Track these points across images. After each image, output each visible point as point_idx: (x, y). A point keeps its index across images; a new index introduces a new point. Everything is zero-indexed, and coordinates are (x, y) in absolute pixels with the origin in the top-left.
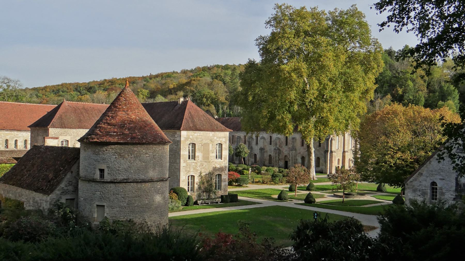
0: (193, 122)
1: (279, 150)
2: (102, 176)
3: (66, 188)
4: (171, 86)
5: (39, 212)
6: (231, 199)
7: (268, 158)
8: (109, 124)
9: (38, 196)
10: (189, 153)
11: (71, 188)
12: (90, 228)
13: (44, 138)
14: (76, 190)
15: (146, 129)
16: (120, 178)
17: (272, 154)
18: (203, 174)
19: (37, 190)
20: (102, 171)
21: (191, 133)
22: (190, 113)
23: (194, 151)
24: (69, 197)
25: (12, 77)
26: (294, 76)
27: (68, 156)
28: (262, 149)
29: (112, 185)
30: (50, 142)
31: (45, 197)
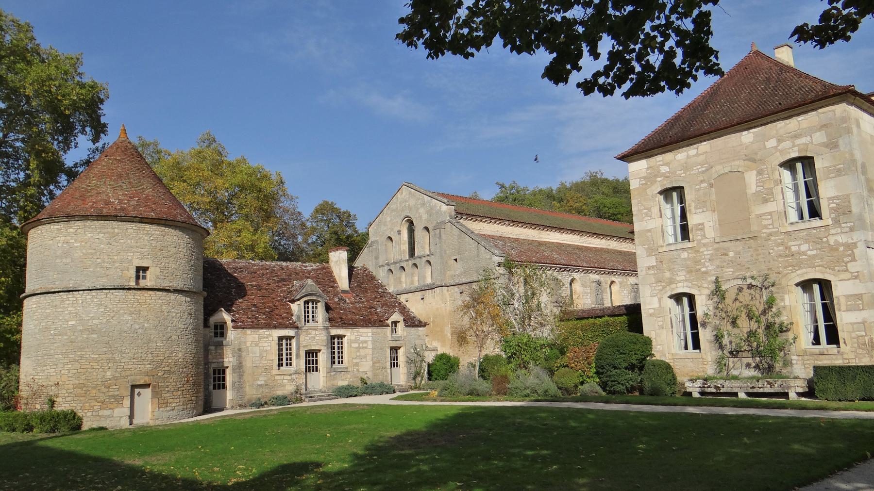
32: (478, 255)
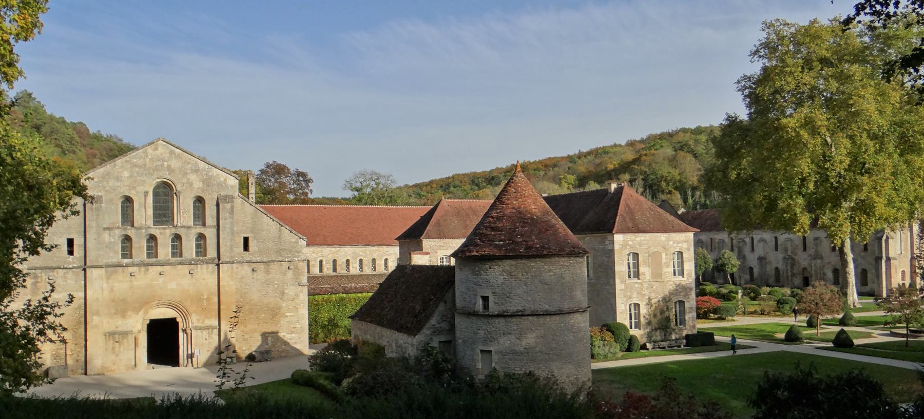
0: (633, 219)
1: (793, 259)
2: (486, 307)
3: (438, 326)
4: (611, 167)
5: (404, 360)
6: (702, 341)
7: (773, 272)
8: (493, 229)
9: (402, 338)
10: (629, 268)
11: (444, 325)
12: (471, 385)
13: (410, 254)
14: (452, 329)
15: (548, 233)
16: (512, 309)
17: (781, 266)
18: (654, 301)
19: (401, 329)
20: (485, 299)
21: (630, 236)
22: (628, 206)
23: (637, 265)
24: (443, 339)
25: (383, 171)
26: (804, 134)
27: (439, 280)
28: (761, 259)
29: (502, 320)
30: (418, 260)
31: (410, 340)
32: (280, 238)
